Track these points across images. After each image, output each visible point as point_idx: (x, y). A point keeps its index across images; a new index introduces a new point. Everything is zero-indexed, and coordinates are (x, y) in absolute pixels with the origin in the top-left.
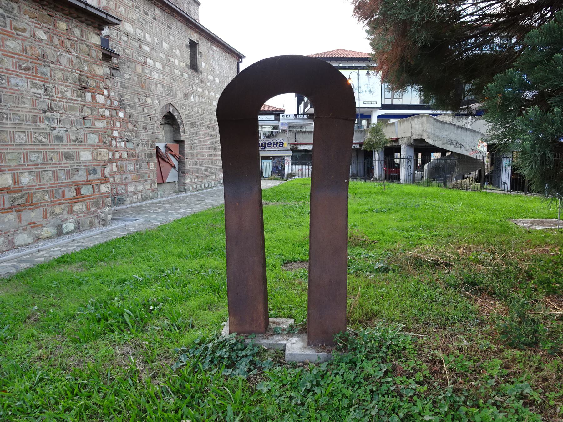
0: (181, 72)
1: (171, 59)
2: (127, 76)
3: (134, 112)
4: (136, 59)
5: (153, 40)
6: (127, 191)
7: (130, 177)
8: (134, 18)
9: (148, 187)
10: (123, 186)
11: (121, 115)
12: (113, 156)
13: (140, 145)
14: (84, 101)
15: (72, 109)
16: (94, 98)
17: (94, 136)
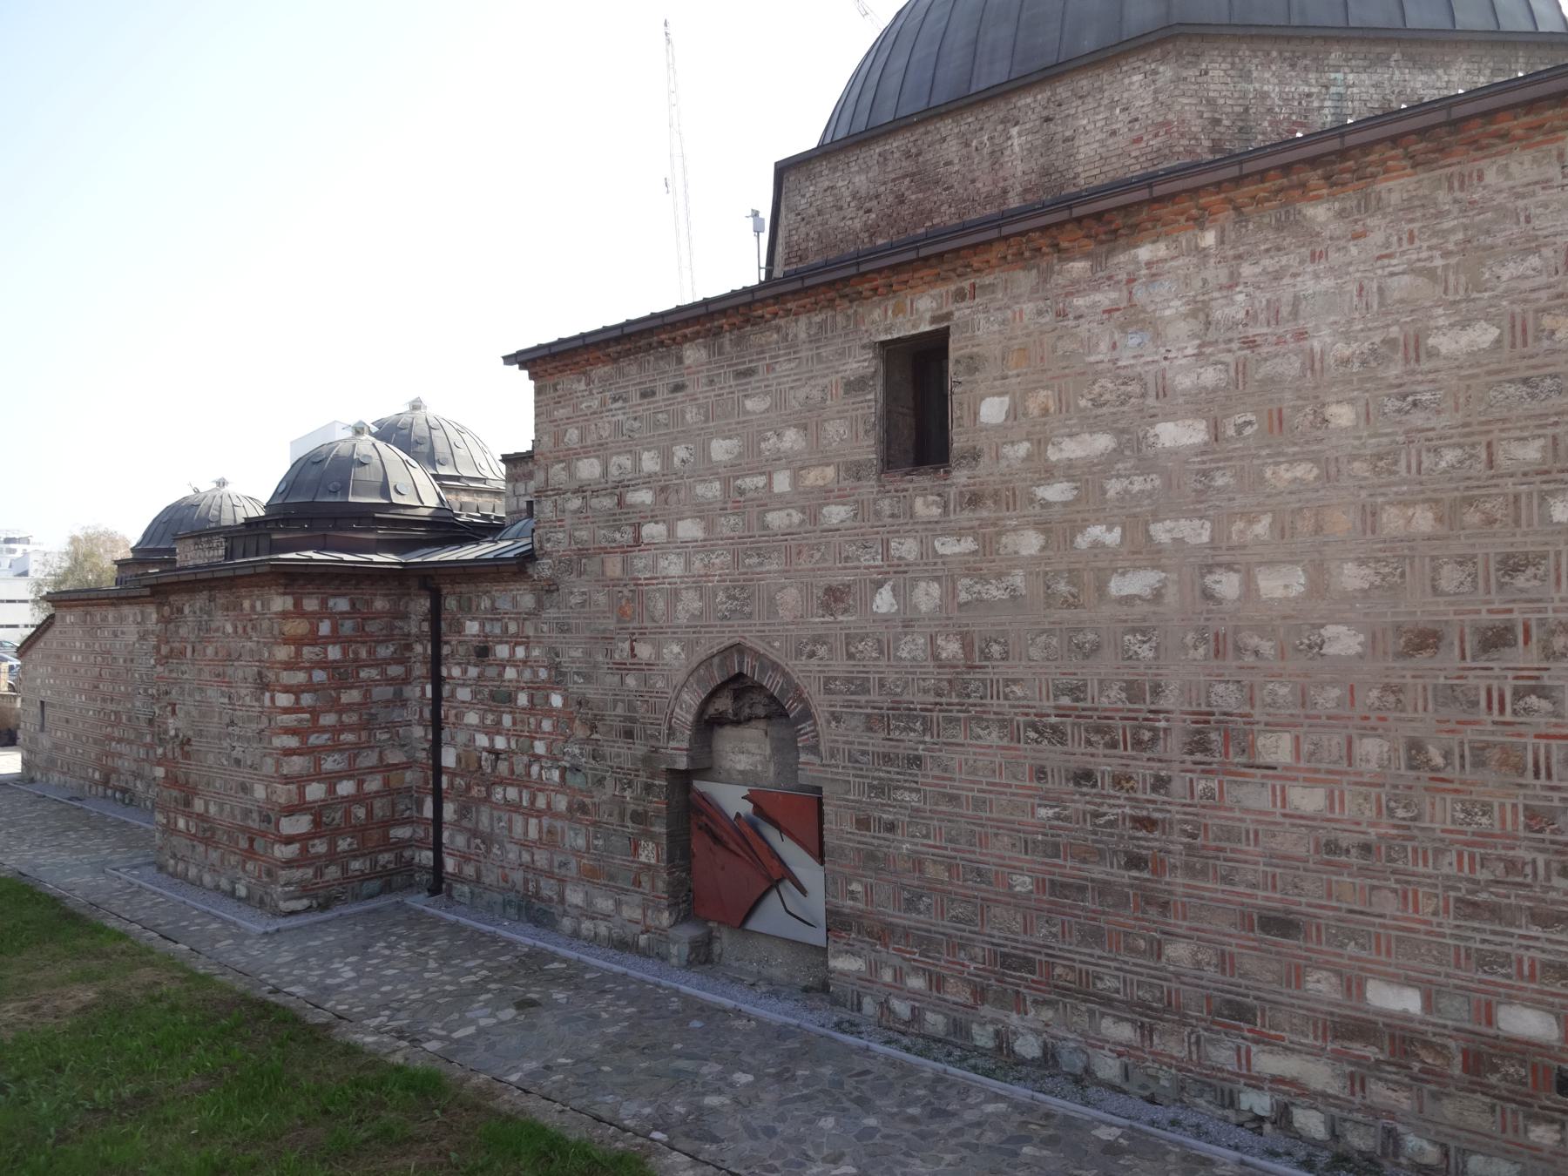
0: (802, 510)
1: (749, 483)
2: (574, 600)
3: (591, 692)
4: (604, 544)
5: (666, 456)
6: (562, 900)
7: (573, 864)
8: (605, 434)
9: (631, 912)
10: (552, 881)
11: (557, 700)
12: (533, 801)
13: (609, 783)
14: (262, 707)
15: (250, 719)
16: (273, 699)
17: (269, 761)
